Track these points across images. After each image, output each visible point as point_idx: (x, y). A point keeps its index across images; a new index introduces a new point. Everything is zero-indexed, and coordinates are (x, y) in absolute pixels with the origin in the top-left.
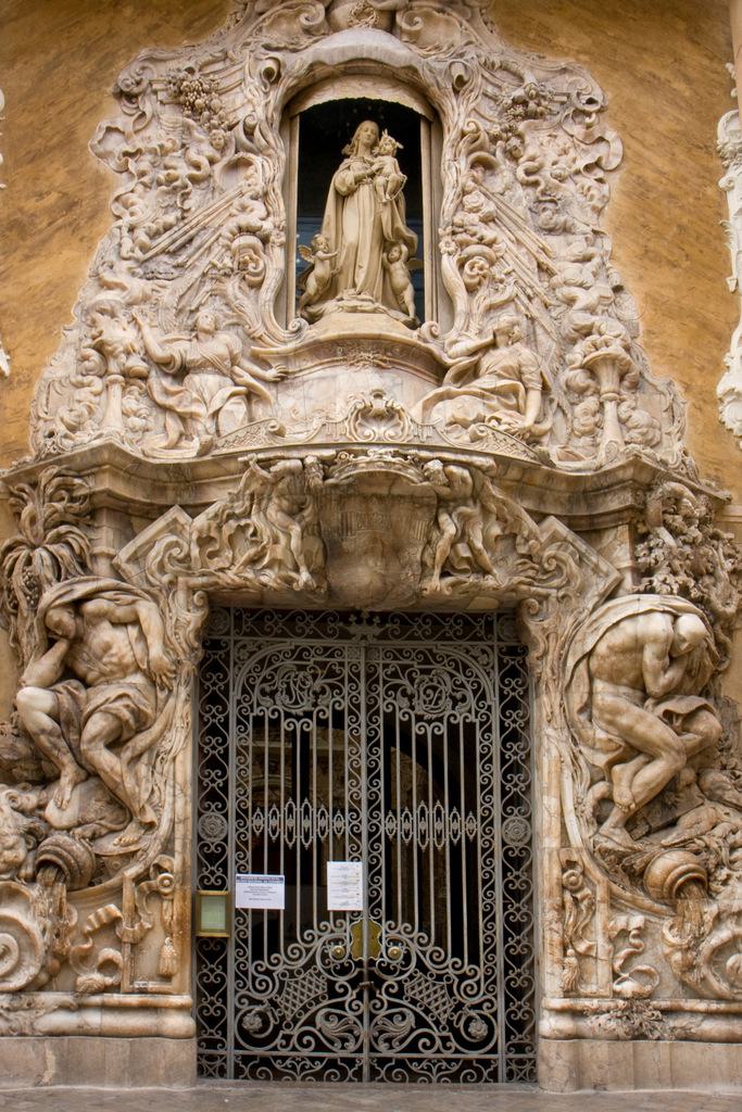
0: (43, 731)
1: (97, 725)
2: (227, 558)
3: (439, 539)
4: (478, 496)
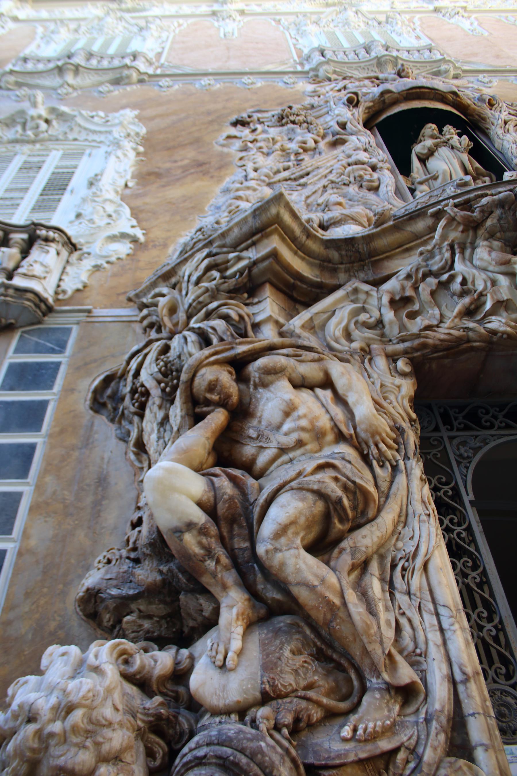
0: (190, 526)
1: (286, 509)
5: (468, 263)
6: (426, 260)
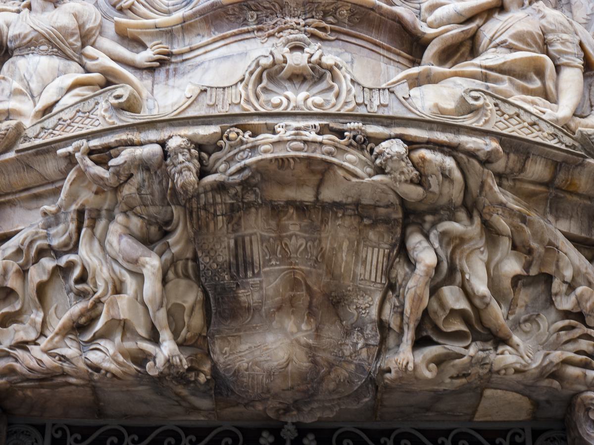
2: (33, 324)
3: (407, 278)
4: (475, 204)
5: (96, 244)
6: (48, 226)
